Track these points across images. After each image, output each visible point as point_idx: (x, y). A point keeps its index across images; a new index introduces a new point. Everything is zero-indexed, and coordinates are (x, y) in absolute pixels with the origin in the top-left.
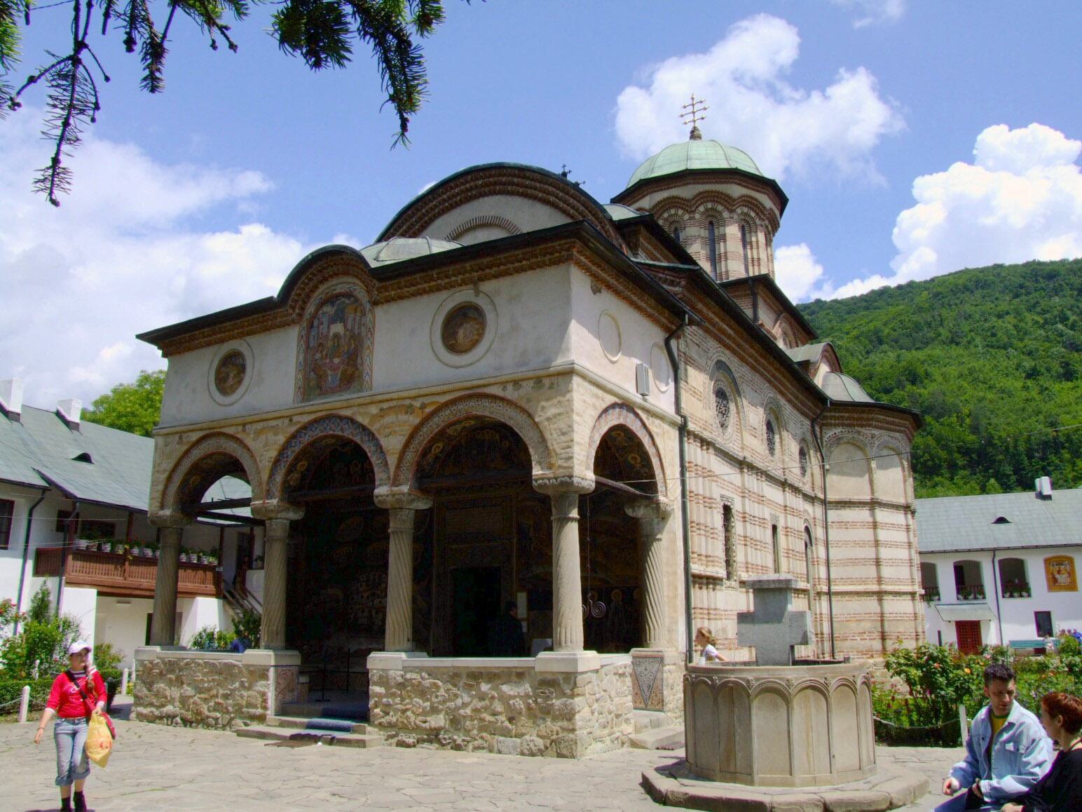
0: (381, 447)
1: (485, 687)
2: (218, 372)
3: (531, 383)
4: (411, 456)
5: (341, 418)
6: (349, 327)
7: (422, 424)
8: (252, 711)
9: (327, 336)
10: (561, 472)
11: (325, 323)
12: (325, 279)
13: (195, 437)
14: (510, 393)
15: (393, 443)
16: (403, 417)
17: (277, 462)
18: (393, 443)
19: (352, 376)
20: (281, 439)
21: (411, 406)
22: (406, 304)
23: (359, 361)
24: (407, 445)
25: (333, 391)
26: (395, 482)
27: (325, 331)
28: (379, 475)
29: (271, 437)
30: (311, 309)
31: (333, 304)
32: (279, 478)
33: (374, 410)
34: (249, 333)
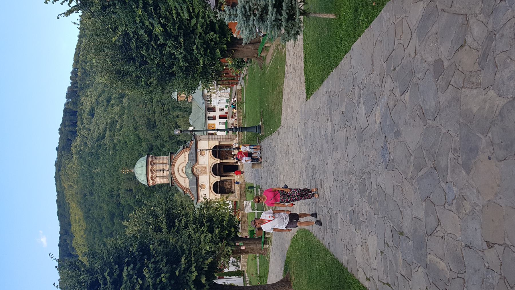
15: (214, 161)
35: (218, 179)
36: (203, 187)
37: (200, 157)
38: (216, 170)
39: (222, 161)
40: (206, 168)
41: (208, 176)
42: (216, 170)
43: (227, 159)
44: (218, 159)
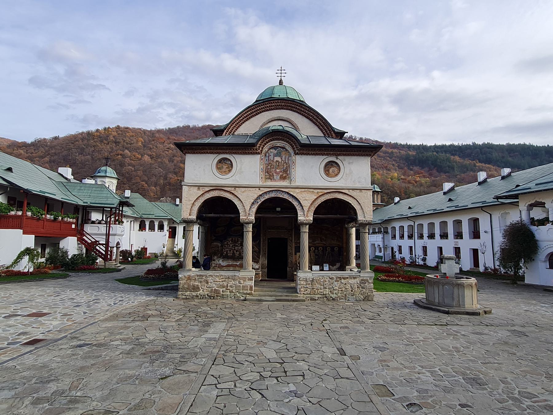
0: (300, 203)
1: (343, 281)
2: (217, 164)
3: (358, 191)
4: (313, 209)
5: (282, 191)
6: (283, 159)
7: (317, 198)
8: (245, 292)
9: (273, 161)
10: (368, 219)
11: (272, 157)
12: (274, 140)
13: (207, 189)
14: (351, 193)
17: (253, 203)
18: (306, 204)
20: (256, 196)
21: (313, 192)
22: (308, 156)
23: (288, 172)
24: (311, 204)
27: (272, 159)
28: (300, 213)
30: (266, 149)
31: (275, 149)
32: (254, 210)
33: (297, 190)
34: (235, 153)
36: (225, 166)
40: (283, 178)
41: (258, 182)
44: (310, 218)
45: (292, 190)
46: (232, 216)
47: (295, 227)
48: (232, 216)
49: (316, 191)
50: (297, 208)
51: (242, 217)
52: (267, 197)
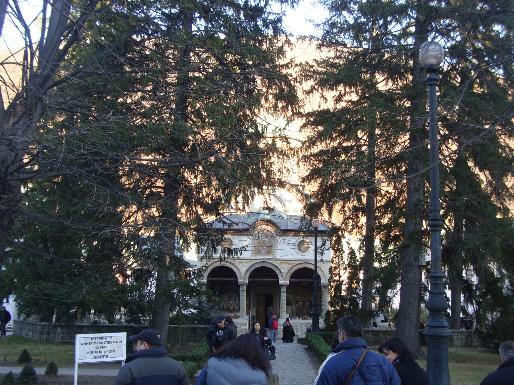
4: (289, 275)
15: (285, 271)
16: (287, 265)
17: (247, 271)
18: (285, 271)
19: (270, 250)
20: (249, 266)
24: (288, 272)
25: (264, 255)
26: (285, 280)
28: (280, 278)
29: (245, 264)
32: (248, 275)
33: (279, 262)
35: (243, 279)
37: (293, 240)
38: (264, 275)
39: (284, 290)
42: (264, 275)
43: (289, 303)
45: (275, 261)
46: (232, 279)
47: (278, 287)
48: (232, 279)
49: (292, 262)
50: (278, 274)
51: (240, 281)
52: (257, 266)
